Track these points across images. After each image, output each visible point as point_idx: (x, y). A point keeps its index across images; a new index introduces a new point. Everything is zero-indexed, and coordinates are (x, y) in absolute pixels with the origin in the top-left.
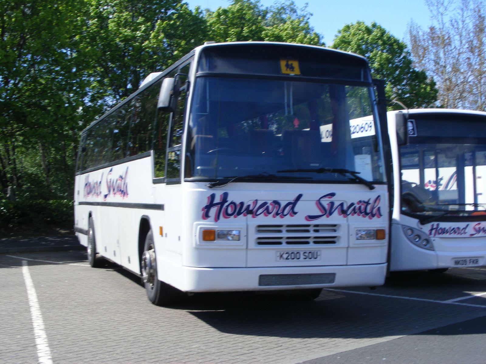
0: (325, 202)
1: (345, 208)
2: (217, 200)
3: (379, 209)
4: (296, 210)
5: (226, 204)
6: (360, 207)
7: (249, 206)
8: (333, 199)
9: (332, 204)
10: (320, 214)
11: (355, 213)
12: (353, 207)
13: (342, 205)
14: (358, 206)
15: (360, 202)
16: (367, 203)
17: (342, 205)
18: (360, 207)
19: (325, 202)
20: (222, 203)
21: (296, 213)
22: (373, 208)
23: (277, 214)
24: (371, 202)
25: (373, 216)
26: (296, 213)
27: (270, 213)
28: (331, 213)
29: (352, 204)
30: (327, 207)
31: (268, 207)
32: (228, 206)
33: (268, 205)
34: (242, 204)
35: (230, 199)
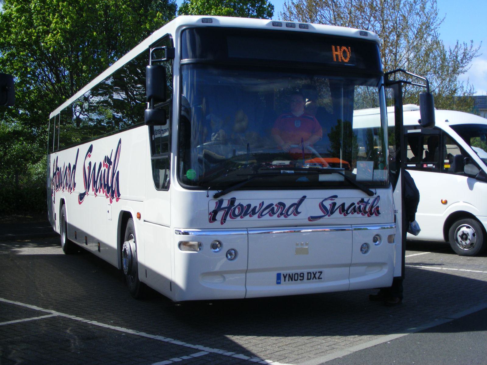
0: (328, 204)
4: (299, 210)
7: (255, 207)
8: (336, 200)
9: (334, 204)
10: (323, 214)
11: (355, 211)
12: (353, 207)
13: (343, 205)
14: (357, 206)
17: (343, 205)
18: (360, 207)
19: (328, 204)
22: (372, 207)
23: (281, 214)
25: (371, 214)
26: (299, 213)
27: (274, 213)
28: (332, 213)
29: (353, 204)
30: (328, 207)
31: (273, 208)
33: (274, 206)
34: (249, 206)
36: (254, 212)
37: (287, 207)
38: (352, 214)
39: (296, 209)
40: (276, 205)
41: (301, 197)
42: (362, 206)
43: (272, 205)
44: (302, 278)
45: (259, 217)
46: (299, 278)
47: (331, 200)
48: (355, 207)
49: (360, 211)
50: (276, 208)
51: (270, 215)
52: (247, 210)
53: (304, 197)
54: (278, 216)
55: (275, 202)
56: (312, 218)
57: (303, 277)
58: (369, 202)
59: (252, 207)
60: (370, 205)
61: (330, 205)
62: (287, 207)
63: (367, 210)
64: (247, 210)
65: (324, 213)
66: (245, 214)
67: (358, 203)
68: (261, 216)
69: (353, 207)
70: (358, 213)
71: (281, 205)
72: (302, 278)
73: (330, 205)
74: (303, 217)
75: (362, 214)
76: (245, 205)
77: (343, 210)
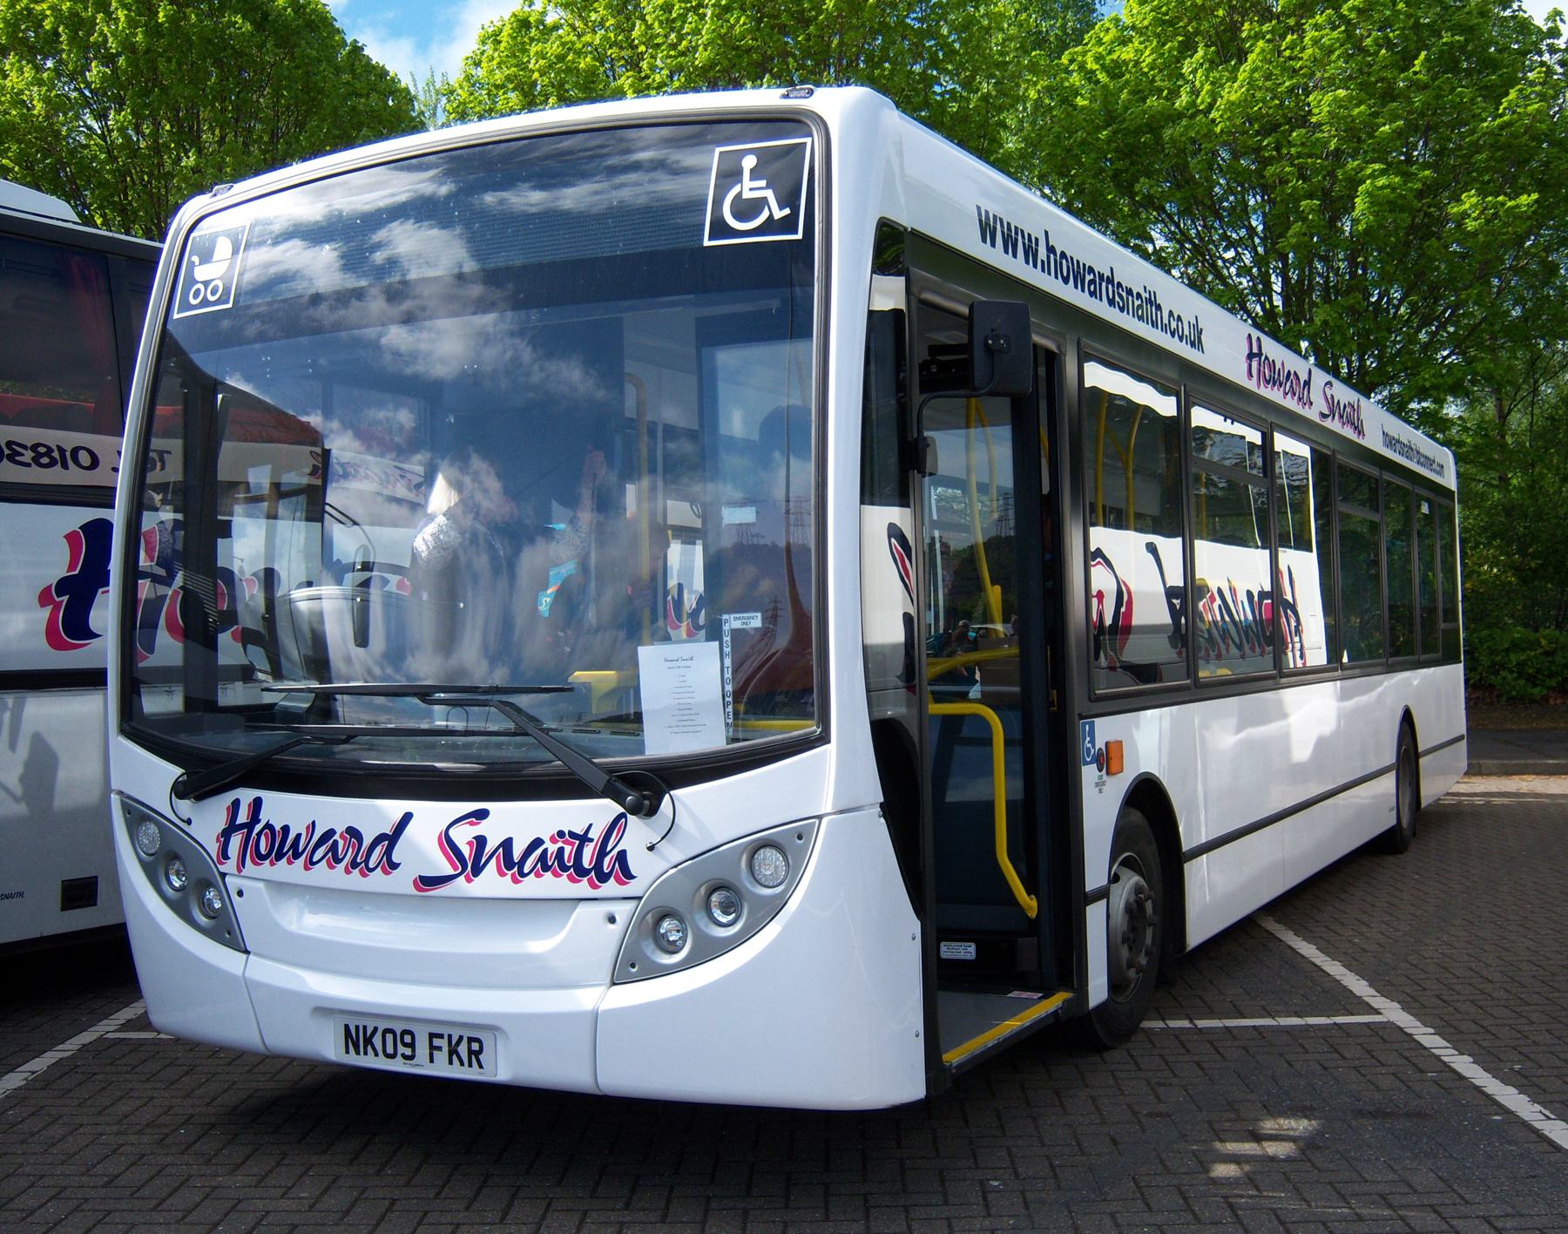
0: (463, 836)
1: (517, 856)
2: (242, 817)
3: (622, 856)
5: (258, 828)
6: (561, 850)
7: (299, 836)
8: (482, 828)
9: (481, 841)
10: (451, 872)
11: (546, 868)
12: (539, 851)
13: (507, 844)
14: (552, 848)
15: (561, 834)
16: (584, 839)
17: (507, 844)
18: (561, 850)
19: (463, 836)
20: (249, 826)
21: (395, 866)
22: (602, 853)
23: (354, 864)
24: (595, 834)
25: (603, 878)
26: (395, 866)
27: (338, 861)
28: (477, 870)
29: (537, 842)
30: (466, 851)
31: (336, 842)
32: (259, 835)
33: (336, 837)
34: (286, 829)
35: (264, 817)
36: (297, 855)
37: (367, 842)
38: (538, 875)
39: (388, 852)
40: (342, 836)
41: (397, 817)
42: (568, 849)
43: (331, 832)
44: (408, 1052)
45: (307, 868)
46: (401, 1049)
47: (472, 824)
48: (546, 850)
49: (564, 868)
50: (341, 843)
51: (331, 867)
52: (282, 846)
53: (408, 817)
54: (347, 872)
55: (340, 829)
56: (428, 882)
57: (412, 1045)
58: (590, 835)
59: (292, 836)
60: (592, 845)
61: (470, 843)
62: (367, 842)
63: (586, 863)
64: (282, 846)
65: (455, 868)
66: (279, 857)
67: (553, 840)
68: (310, 863)
69: (539, 851)
70: (557, 875)
71: (353, 833)
72: (408, 1052)
73: (470, 843)
74: (401, 881)
75: (571, 878)
76: (278, 828)
77: (509, 861)
